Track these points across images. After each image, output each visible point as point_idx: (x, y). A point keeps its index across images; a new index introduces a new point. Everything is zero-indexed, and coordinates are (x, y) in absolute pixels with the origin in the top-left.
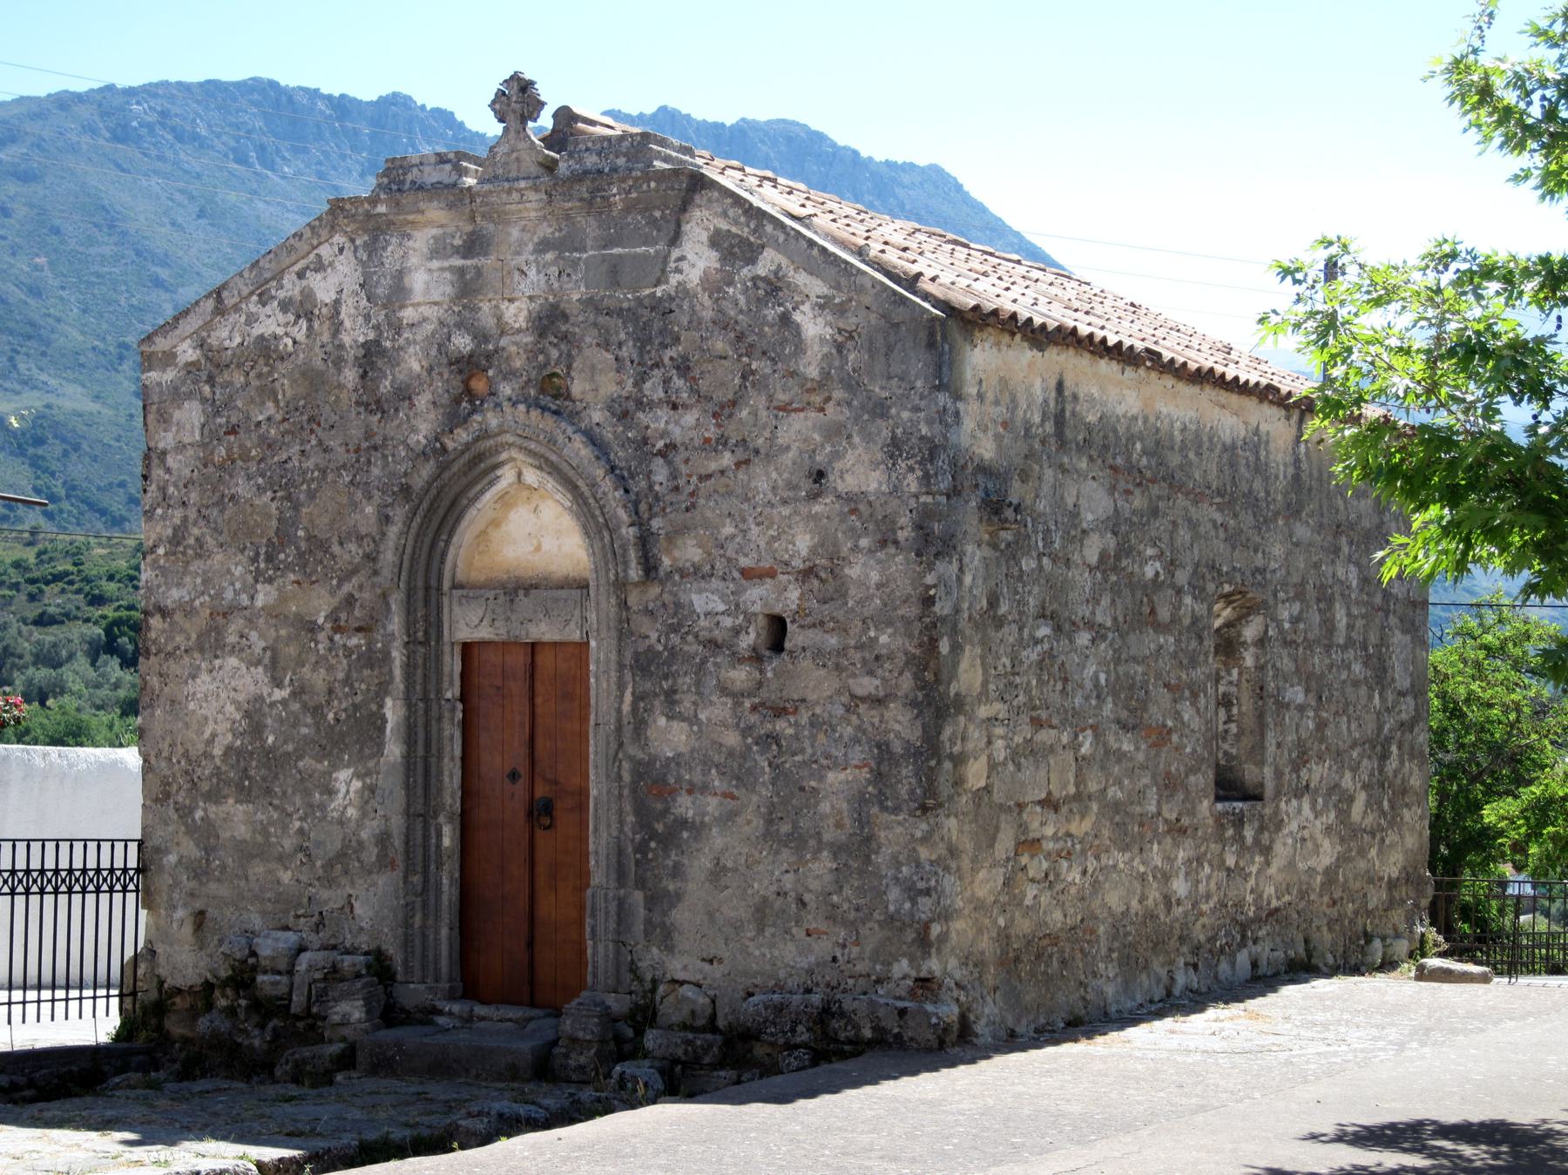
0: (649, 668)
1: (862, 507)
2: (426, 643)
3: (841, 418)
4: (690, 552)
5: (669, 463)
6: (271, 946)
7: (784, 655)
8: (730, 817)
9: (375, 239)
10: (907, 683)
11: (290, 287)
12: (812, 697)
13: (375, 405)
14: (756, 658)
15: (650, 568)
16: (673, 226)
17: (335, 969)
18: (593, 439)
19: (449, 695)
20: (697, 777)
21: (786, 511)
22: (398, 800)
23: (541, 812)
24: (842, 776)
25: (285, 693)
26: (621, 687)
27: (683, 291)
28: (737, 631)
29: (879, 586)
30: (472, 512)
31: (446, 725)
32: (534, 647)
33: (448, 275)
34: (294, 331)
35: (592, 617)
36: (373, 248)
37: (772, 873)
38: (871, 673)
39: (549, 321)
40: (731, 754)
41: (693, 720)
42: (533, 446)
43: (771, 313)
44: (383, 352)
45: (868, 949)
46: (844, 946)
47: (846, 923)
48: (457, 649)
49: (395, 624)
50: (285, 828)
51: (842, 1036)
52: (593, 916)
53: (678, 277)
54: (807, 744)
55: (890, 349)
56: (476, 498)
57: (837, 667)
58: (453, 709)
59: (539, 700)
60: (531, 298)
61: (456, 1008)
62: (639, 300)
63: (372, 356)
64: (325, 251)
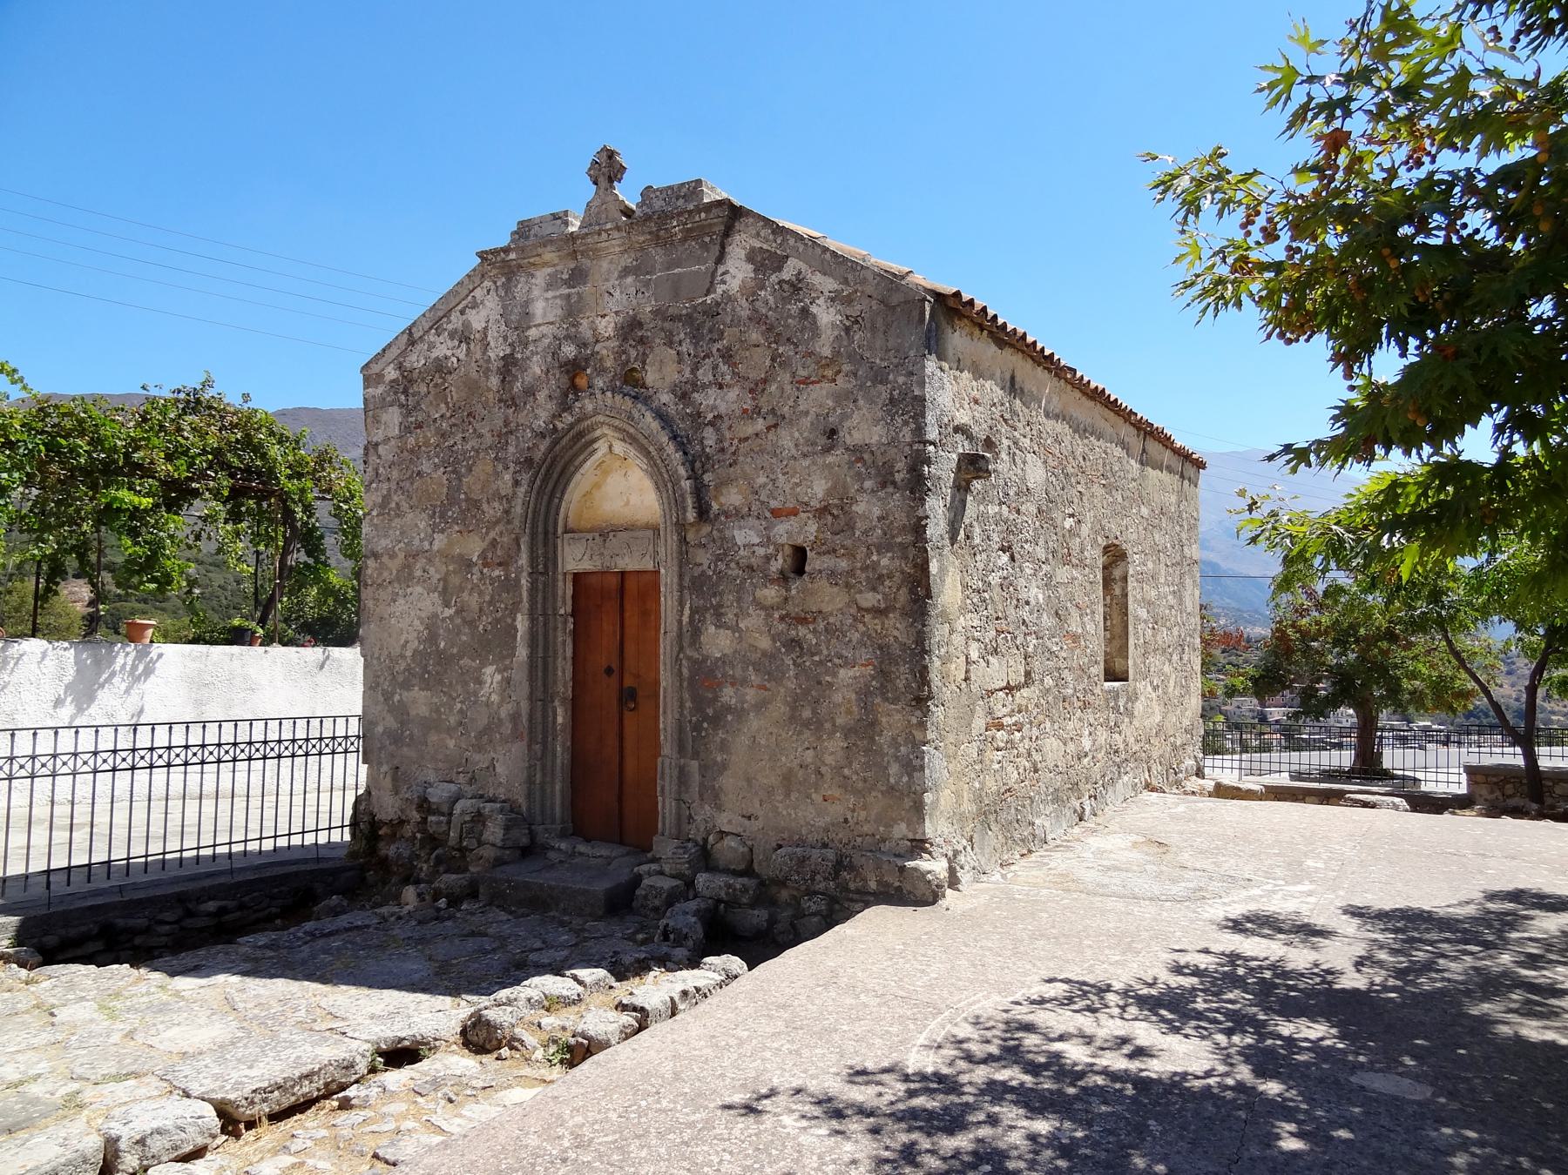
0: (697, 585)
1: (866, 456)
2: (545, 573)
3: (850, 386)
4: (733, 497)
5: (718, 430)
6: (439, 794)
7: (805, 577)
8: (761, 706)
9: (509, 280)
10: (903, 596)
11: (456, 321)
12: (827, 609)
13: (511, 402)
14: (783, 578)
15: (703, 512)
16: (717, 247)
17: (479, 813)
18: (662, 416)
19: (562, 611)
20: (738, 672)
21: (806, 463)
22: (524, 689)
23: (628, 697)
24: (851, 673)
25: (452, 611)
26: (681, 604)
27: (728, 298)
28: (768, 558)
29: (880, 519)
30: (578, 476)
31: (560, 633)
32: (623, 573)
33: (558, 301)
34: (458, 352)
35: (662, 550)
36: (507, 287)
37: (798, 752)
38: (874, 589)
39: (631, 328)
40: (764, 654)
41: (735, 628)
42: (617, 423)
43: (794, 308)
44: (515, 362)
45: (873, 814)
46: (853, 811)
47: (857, 792)
48: (570, 578)
49: (523, 560)
50: (451, 709)
51: (852, 886)
52: (663, 778)
53: (723, 287)
54: (823, 647)
55: (888, 326)
56: (581, 465)
57: (847, 585)
58: (565, 622)
59: (627, 615)
60: (616, 313)
61: (563, 846)
62: (695, 307)
63: (509, 365)
64: (478, 293)
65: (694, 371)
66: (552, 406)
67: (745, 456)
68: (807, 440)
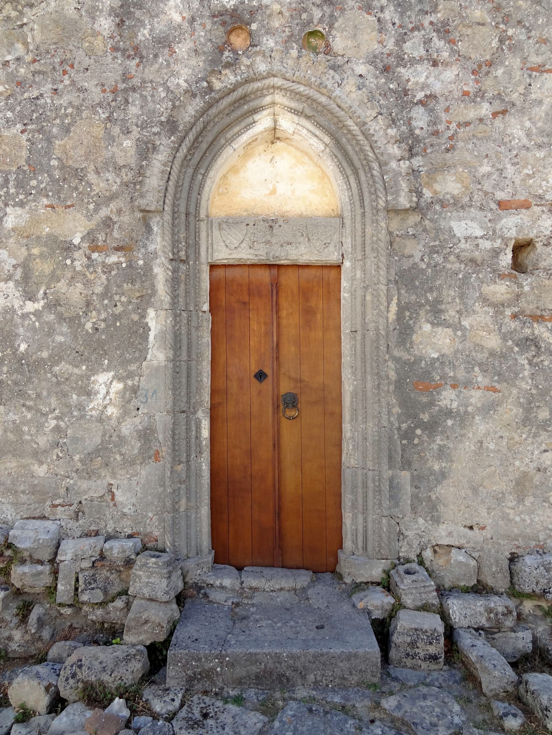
65: (401, 40)
66: (199, 63)
67: (467, 141)
68: (541, 132)
